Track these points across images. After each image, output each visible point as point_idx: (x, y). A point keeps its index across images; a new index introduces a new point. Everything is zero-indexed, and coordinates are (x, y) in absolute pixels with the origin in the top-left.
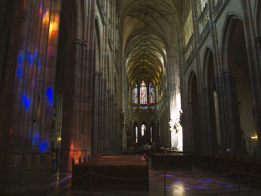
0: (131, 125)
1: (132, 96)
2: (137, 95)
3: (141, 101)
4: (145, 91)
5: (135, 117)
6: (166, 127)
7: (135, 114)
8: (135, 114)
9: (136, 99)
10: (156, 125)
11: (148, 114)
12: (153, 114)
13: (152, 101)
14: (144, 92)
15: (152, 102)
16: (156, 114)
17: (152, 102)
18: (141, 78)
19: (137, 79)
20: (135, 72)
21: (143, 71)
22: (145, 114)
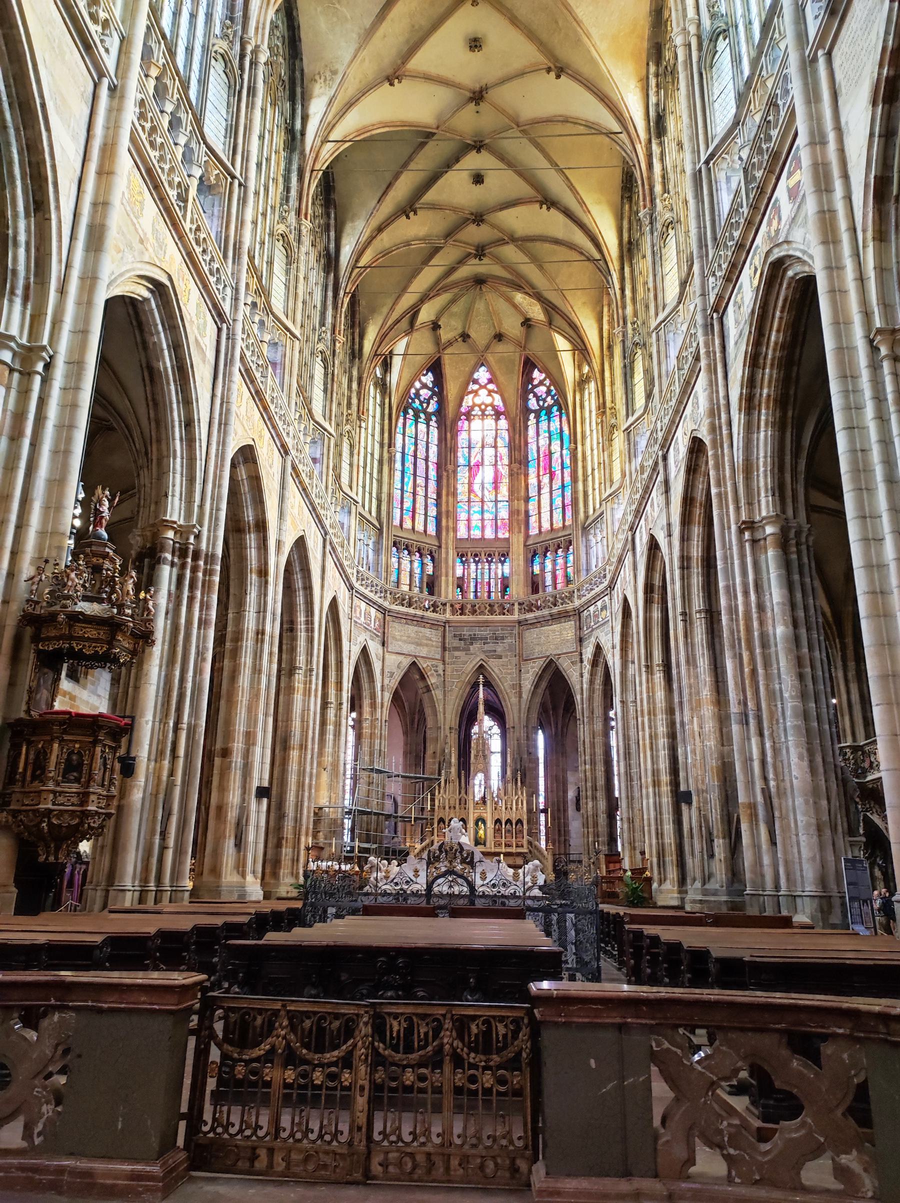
0: (366, 693)
1: (391, 470)
2: (433, 474)
3: (463, 516)
4: (495, 447)
5: (412, 630)
6: (732, 610)
7: (411, 611)
8: (411, 611)
9: (426, 496)
10: (579, 697)
11: (516, 616)
12: (555, 610)
13: (545, 516)
14: (489, 452)
15: (546, 525)
16: (577, 603)
17: (546, 525)
18: (465, 336)
19: (437, 341)
20: (407, 243)
21: (480, 252)
22: (492, 612)
